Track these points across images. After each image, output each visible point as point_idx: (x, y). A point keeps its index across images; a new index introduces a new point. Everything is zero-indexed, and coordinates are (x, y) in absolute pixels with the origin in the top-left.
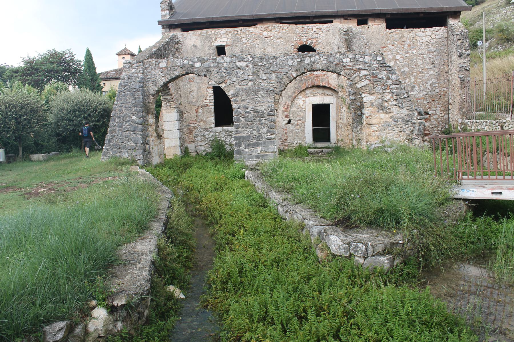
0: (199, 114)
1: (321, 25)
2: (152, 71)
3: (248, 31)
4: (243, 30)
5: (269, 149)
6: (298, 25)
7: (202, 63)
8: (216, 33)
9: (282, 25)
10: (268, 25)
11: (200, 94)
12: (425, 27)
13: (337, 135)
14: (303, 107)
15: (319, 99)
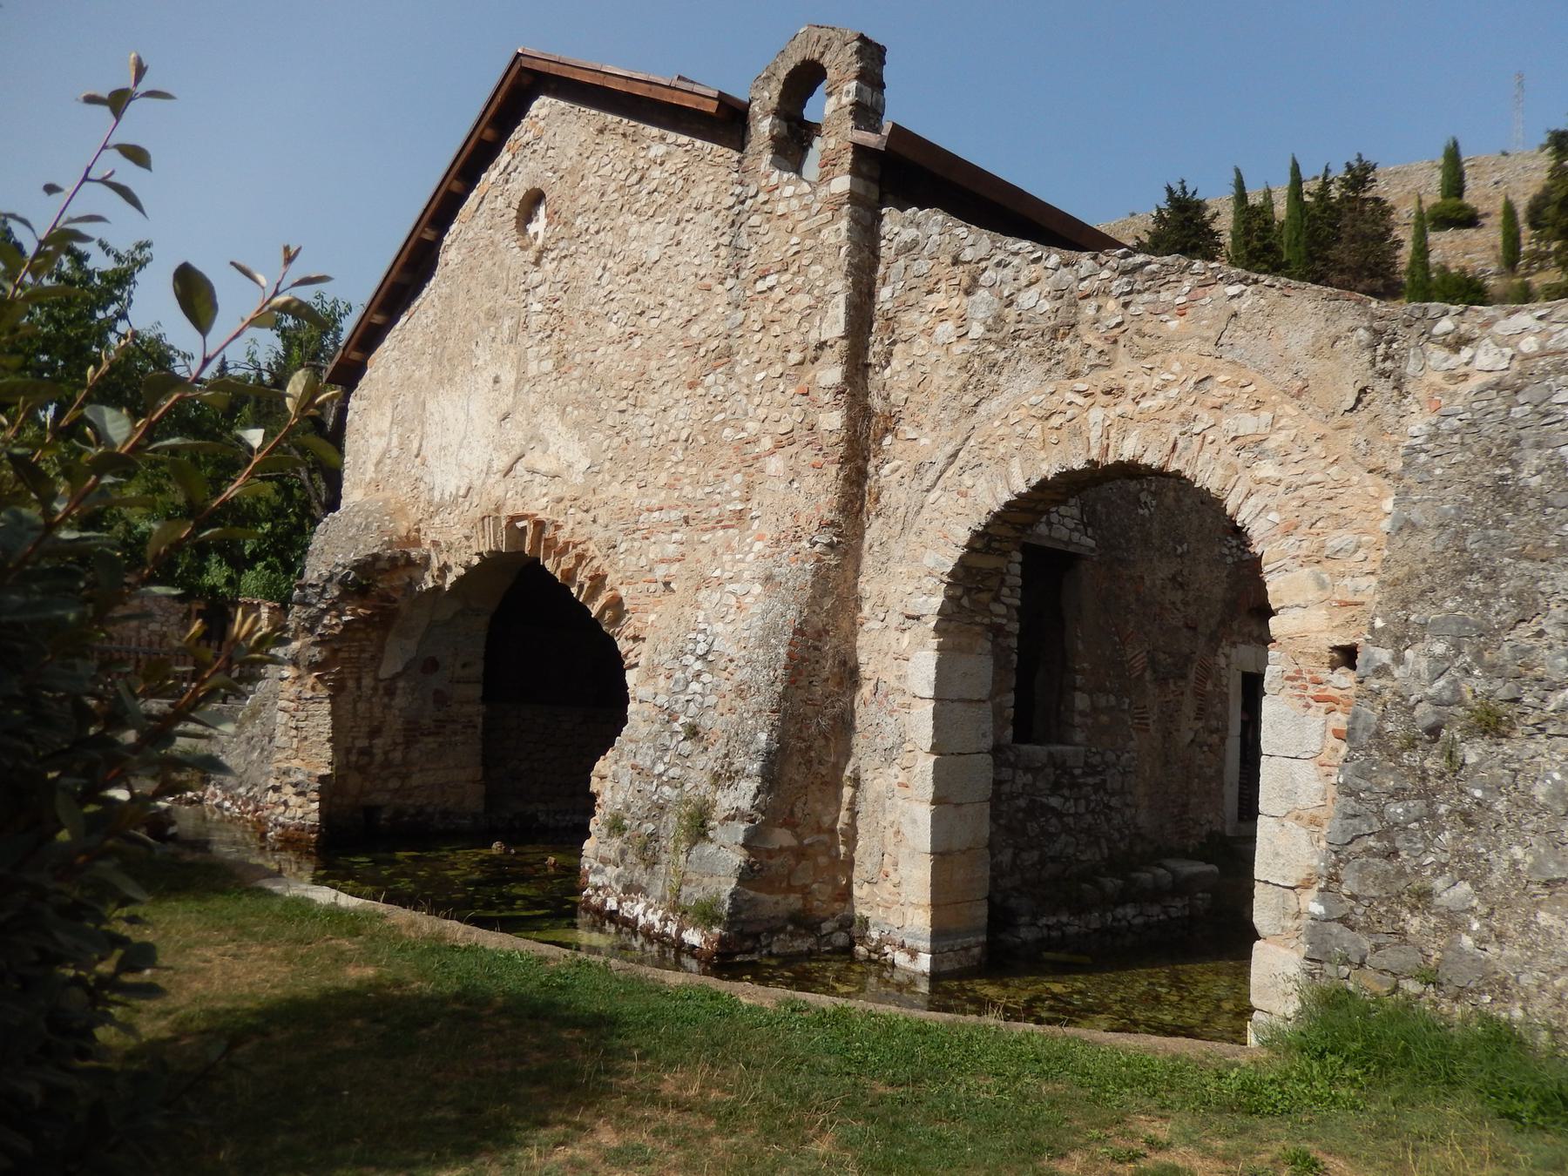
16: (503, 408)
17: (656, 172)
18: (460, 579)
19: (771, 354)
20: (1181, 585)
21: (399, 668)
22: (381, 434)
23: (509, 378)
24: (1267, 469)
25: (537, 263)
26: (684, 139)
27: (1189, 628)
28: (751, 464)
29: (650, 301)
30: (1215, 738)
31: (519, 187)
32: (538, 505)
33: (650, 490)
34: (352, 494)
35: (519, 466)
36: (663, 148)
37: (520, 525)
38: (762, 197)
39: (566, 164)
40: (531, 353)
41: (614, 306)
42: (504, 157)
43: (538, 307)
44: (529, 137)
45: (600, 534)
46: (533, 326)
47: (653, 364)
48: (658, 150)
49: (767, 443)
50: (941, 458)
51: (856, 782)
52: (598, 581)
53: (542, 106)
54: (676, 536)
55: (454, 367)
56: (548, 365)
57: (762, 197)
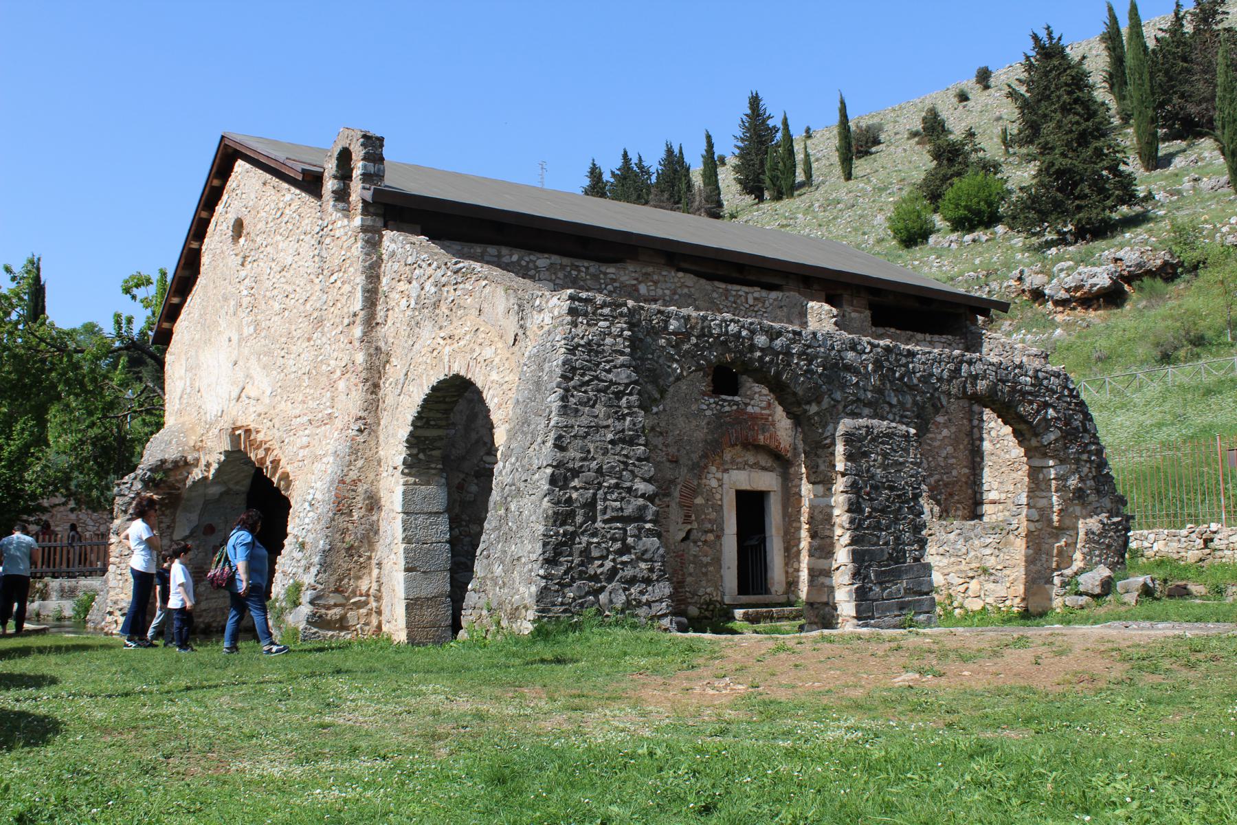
0: (470, 497)
1: (764, 293)
2: (649, 340)
3: (606, 274)
4: (592, 270)
5: (920, 584)
6: (717, 284)
7: (772, 340)
8: (524, 263)
9: (680, 274)
10: (650, 269)
11: (474, 436)
12: (931, 333)
13: (787, 572)
14: (718, 496)
15: (744, 479)
16: (234, 358)
17: (287, 211)
18: (218, 471)
19: (338, 320)
20: (661, 433)
21: (187, 533)
22: (181, 378)
23: (235, 338)
24: (494, 376)
25: (243, 265)
26: (298, 192)
27: (671, 461)
28: (333, 385)
29: (289, 288)
30: (711, 537)
31: (231, 218)
32: (249, 420)
33: (296, 404)
34: (170, 420)
35: (243, 395)
36: (292, 194)
37: (237, 432)
38: (330, 227)
39: (251, 203)
40: (244, 322)
41: (276, 292)
42: (225, 197)
43: (245, 292)
44: (234, 185)
45: (277, 434)
46: (244, 305)
47: (293, 327)
48: (288, 197)
49: (338, 373)
50: (402, 376)
51: (379, 564)
52: (276, 463)
53: (240, 166)
54: (307, 432)
55: (211, 332)
56: (252, 329)
57: (330, 227)
